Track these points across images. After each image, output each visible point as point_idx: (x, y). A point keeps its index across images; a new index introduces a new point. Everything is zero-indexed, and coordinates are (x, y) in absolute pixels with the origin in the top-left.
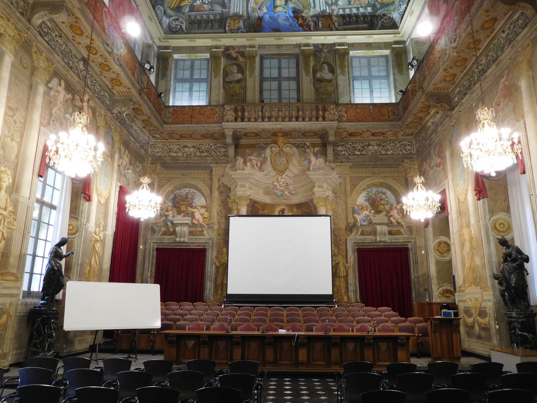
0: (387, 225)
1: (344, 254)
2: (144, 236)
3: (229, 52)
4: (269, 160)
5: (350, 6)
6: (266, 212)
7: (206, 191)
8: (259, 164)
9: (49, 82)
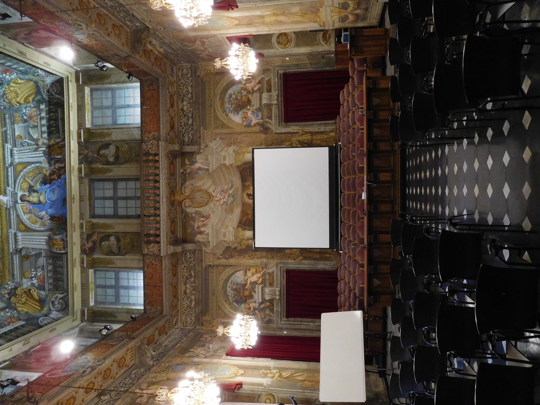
0: (261, 93)
2: (274, 330)
3: (87, 249)
5: (39, 126)
6: (250, 212)
7: (229, 271)
8: (202, 219)
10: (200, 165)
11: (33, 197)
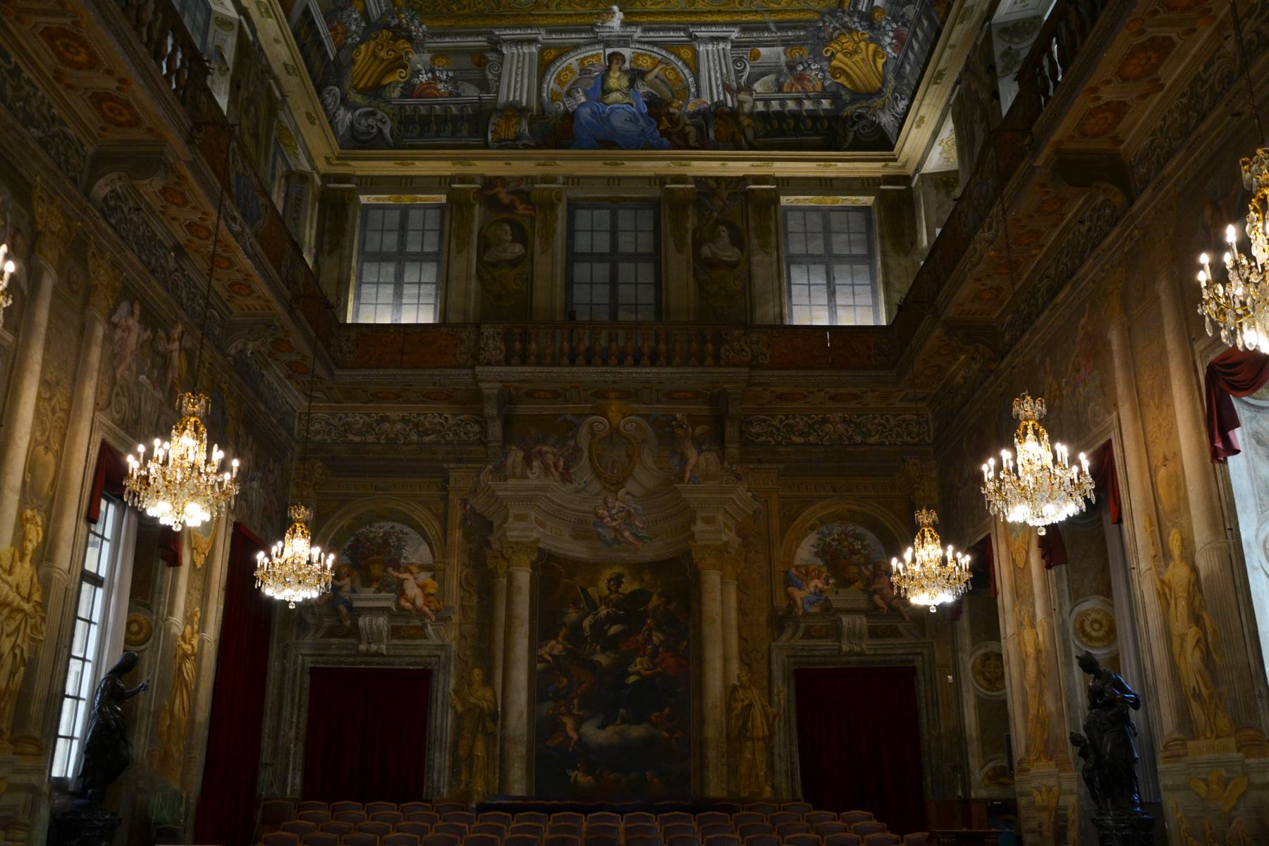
1: (765, 683)
4: (586, 454)
7: (433, 529)
8: (561, 463)
9: (113, 311)
10: (692, 461)
11: (619, 78)
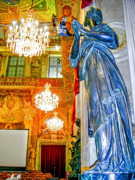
1: (35, 148)
